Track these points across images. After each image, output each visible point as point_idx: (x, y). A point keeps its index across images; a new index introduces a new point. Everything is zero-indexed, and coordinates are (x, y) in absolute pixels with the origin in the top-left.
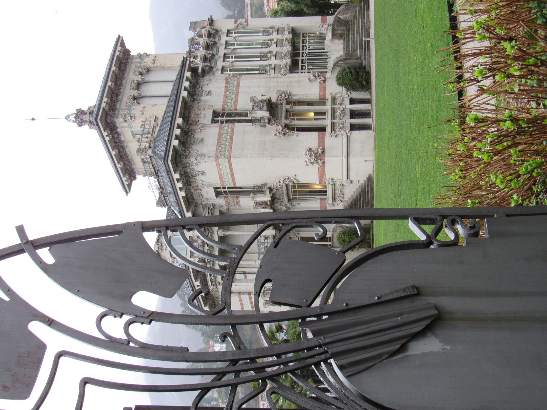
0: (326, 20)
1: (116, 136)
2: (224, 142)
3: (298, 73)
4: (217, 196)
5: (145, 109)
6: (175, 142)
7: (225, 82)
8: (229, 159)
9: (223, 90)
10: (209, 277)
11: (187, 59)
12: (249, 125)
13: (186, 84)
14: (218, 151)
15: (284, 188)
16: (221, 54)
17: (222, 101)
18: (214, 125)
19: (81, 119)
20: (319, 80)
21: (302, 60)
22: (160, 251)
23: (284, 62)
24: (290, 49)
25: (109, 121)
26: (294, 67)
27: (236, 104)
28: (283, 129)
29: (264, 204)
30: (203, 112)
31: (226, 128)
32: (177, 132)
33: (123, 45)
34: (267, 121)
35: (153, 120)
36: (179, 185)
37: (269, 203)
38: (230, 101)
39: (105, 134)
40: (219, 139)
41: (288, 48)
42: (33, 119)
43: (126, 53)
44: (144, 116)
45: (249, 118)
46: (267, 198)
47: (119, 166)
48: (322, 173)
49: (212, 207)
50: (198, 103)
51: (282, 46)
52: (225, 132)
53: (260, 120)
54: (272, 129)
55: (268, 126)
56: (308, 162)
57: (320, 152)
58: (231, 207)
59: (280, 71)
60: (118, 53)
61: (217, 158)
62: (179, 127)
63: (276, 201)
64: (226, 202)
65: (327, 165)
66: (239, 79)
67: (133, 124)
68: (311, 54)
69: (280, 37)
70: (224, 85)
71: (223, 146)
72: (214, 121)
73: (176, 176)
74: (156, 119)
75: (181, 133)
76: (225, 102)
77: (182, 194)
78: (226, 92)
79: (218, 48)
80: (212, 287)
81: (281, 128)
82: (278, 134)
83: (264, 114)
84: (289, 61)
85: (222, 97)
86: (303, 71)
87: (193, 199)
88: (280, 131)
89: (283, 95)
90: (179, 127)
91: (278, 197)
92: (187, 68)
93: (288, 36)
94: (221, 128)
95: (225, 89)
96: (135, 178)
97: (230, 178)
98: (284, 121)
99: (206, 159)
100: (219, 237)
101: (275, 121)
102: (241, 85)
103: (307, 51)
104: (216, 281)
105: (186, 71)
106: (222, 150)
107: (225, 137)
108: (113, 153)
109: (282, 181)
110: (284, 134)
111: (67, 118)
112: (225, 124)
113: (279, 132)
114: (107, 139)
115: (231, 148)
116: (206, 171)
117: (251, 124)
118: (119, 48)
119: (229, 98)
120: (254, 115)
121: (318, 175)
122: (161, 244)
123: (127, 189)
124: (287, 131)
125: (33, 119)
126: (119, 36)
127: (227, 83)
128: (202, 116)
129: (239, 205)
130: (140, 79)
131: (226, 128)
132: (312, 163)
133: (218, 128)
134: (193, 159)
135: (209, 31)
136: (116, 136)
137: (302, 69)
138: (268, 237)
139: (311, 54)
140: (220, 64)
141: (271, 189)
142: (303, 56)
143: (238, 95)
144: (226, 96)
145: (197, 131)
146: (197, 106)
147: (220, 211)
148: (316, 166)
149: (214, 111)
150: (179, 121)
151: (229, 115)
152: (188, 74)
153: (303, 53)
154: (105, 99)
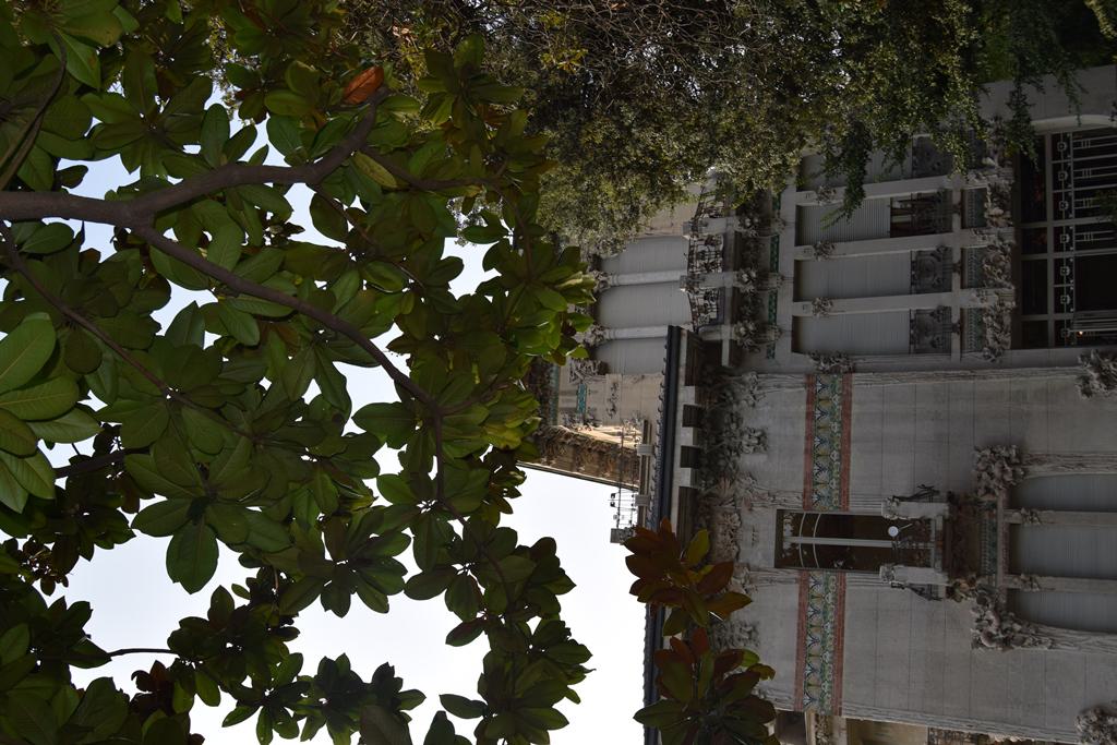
2: (816, 648)
5: (619, 393)
9: (801, 428)
16: (786, 267)
17: (801, 476)
18: (782, 574)
21: (1058, 263)
23: (990, 300)
27: (844, 494)
28: (1001, 620)
30: (749, 520)
31: (819, 590)
38: (823, 476)
40: (803, 630)
41: (998, 236)
50: (732, 483)
51: (980, 224)
66: (847, 383)
68: (1088, 237)
69: (976, 182)
70: (803, 408)
71: (816, 664)
72: (785, 559)
76: (810, 480)
78: (809, 437)
79: (775, 241)
85: (801, 459)
88: (992, 629)
89: (996, 470)
92: (682, 371)
94: (804, 584)
95: (808, 426)
101: (971, 582)
102: (855, 409)
103: (1073, 222)
105: (682, 382)
113: (990, 637)
115: (839, 671)
119: (823, 462)
124: (1017, 627)
127: (812, 399)
128: (747, 536)
131: (819, 590)
133: (795, 588)
139: (1088, 237)
140: (787, 309)
142: (1058, 247)
143: (849, 452)
144: (811, 453)
146: (728, 492)
153: (1058, 231)
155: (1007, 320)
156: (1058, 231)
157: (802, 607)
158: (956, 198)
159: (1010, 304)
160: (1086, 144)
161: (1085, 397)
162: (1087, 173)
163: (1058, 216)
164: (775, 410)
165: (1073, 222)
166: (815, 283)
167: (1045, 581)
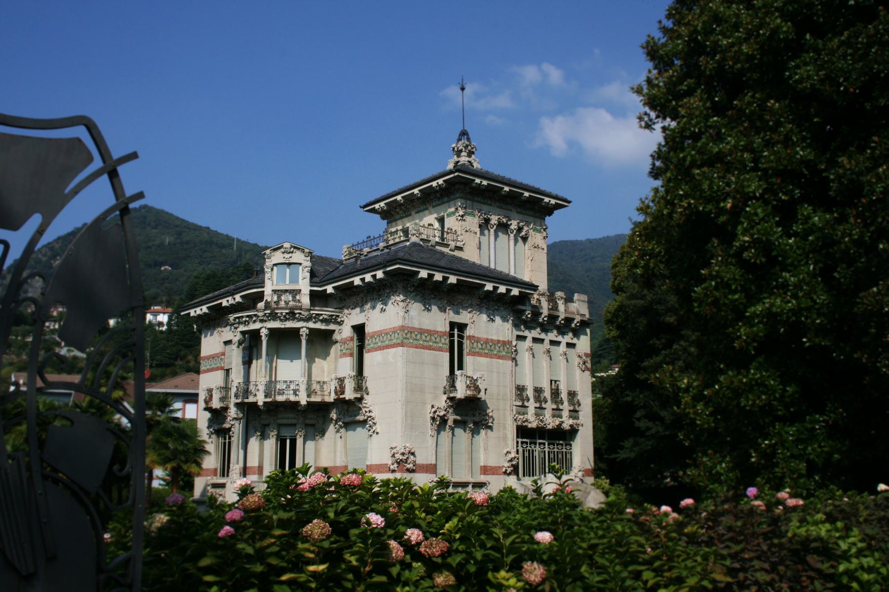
0: (589, 475)
1: (438, 195)
2: (424, 337)
3: (517, 437)
4: (353, 327)
6: (424, 274)
7: (506, 340)
8: (402, 345)
9: (495, 338)
11: (535, 290)
12: (447, 372)
13: (502, 289)
14: (411, 330)
15: (361, 418)
19: (461, 151)
20: (507, 464)
22: (282, 250)
24: (550, 427)
25: (457, 186)
26: (523, 432)
29: (341, 390)
31: (443, 340)
32: (438, 277)
33: (558, 207)
34: (452, 395)
35: (459, 244)
36: (368, 278)
37: (342, 396)
38: (480, 346)
39: (440, 181)
40: (430, 333)
41: (551, 423)
42: (463, 89)
43: (549, 210)
44: (463, 232)
45: (457, 372)
46: (349, 394)
47: (399, 198)
49: (339, 320)
51: (554, 416)
52: (438, 340)
53: (453, 386)
54: (442, 401)
55: (445, 397)
56: (395, 451)
57: (409, 466)
58: (338, 345)
59: (519, 414)
60: (547, 200)
61: (402, 328)
62: (445, 279)
63: (346, 407)
64: (346, 339)
67: (453, 218)
69: (565, 414)
70: (501, 339)
71: (418, 337)
72: (453, 325)
73: (380, 274)
74: (460, 249)
75: (437, 281)
76: (478, 340)
77: (357, 281)
80: (232, 319)
81: (442, 414)
82: (433, 410)
83: (461, 392)
84: (533, 425)
85: (485, 336)
86: (520, 444)
87: (350, 295)
90: (445, 279)
91: (350, 409)
93: (567, 423)
94: (444, 334)
96: (383, 219)
97: (376, 346)
98: (451, 418)
99: (402, 313)
100: (298, 329)
102: (501, 361)
103: (547, 450)
104: (239, 323)
106: (413, 335)
107: (431, 339)
108: (416, 191)
109: (370, 414)
110: (433, 419)
111: (464, 134)
112: (447, 341)
113: (435, 412)
115: (416, 347)
117: (448, 374)
118: (553, 201)
120: (459, 378)
122: (292, 252)
123: (368, 207)
125: (463, 89)
126: (569, 202)
129: (341, 357)
130: (512, 227)
131: (443, 340)
132: (393, 456)
134: (402, 297)
135: (573, 319)
136: (438, 195)
137: (522, 443)
138: (296, 395)
140: (530, 334)
141: (360, 400)
142: (540, 444)
144: (487, 341)
145: (439, 302)
146: (474, 303)
147: (334, 331)
148: (389, 461)
149: (466, 325)
150: (453, 279)
151: (460, 345)
152: (515, 292)
154: (485, 183)
155: (526, 424)
156: (544, 444)
157: (437, 332)
158: (561, 407)
159: (530, 426)
160: (568, 456)
161: (505, 451)
162: (560, 456)
163: (549, 444)
164: (501, 329)
165: (547, 450)
166: (538, 347)
167: (450, 433)
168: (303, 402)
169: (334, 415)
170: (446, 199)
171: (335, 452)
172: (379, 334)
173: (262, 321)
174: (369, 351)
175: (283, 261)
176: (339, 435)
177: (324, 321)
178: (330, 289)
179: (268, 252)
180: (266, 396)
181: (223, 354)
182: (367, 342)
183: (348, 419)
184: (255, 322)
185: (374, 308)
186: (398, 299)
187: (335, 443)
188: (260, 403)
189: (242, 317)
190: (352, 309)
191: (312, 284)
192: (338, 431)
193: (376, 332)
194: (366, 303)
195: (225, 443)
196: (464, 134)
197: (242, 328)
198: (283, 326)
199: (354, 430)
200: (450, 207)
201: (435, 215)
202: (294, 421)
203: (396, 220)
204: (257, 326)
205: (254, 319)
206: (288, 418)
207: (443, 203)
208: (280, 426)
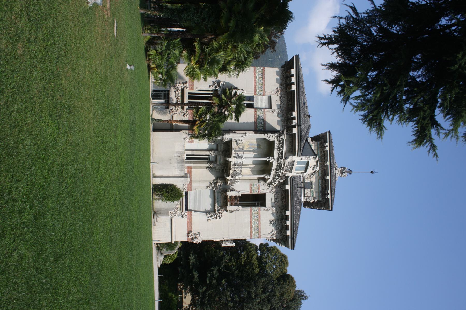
10: (284, 151)
19: (343, 174)
37: (229, 203)
42: (372, 172)
48: (189, 223)
63: (223, 195)
65: (186, 232)
77: (288, 213)
80: (283, 138)
100: (270, 175)
104: (280, 141)
108: (329, 177)
109: (218, 217)
114: (329, 192)
116: (269, 224)
121: (193, 222)
125: (372, 172)
129: (251, 185)
141: (227, 211)
168: (228, 178)
169: (220, 182)
170: (320, 189)
171: (199, 182)
172: (259, 214)
173: (278, 160)
174: (251, 211)
175: (310, 165)
176: (208, 184)
177: (271, 183)
178: (288, 187)
179: (317, 159)
180: (235, 164)
181: (264, 94)
182: (256, 208)
183: (216, 195)
184: (279, 155)
185: (273, 215)
186: (275, 235)
187: (204, 181)
188: (230, 159)
189: (283, 147)
190: (275, 195)
191: (293, 177)
192: (211, 184)
193: (260, 217)
194: (276, 209)
195: (209, 91)
196: (350, 172)
197: (276, 143)
198: (273, 169)
199: (210, 197)
200: (316, 192)
201: (314, 182)
202: (218, 163)
203: (318, 150)
204: (276, 156)
205: (280, 156)
206: (220, 161)
207: (319, 187)
208: (216, 157)
